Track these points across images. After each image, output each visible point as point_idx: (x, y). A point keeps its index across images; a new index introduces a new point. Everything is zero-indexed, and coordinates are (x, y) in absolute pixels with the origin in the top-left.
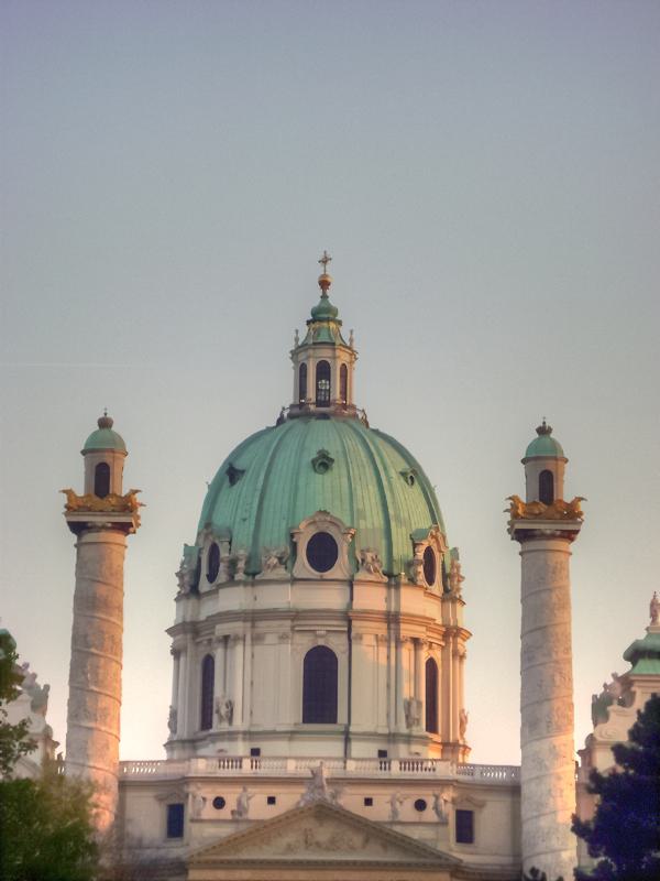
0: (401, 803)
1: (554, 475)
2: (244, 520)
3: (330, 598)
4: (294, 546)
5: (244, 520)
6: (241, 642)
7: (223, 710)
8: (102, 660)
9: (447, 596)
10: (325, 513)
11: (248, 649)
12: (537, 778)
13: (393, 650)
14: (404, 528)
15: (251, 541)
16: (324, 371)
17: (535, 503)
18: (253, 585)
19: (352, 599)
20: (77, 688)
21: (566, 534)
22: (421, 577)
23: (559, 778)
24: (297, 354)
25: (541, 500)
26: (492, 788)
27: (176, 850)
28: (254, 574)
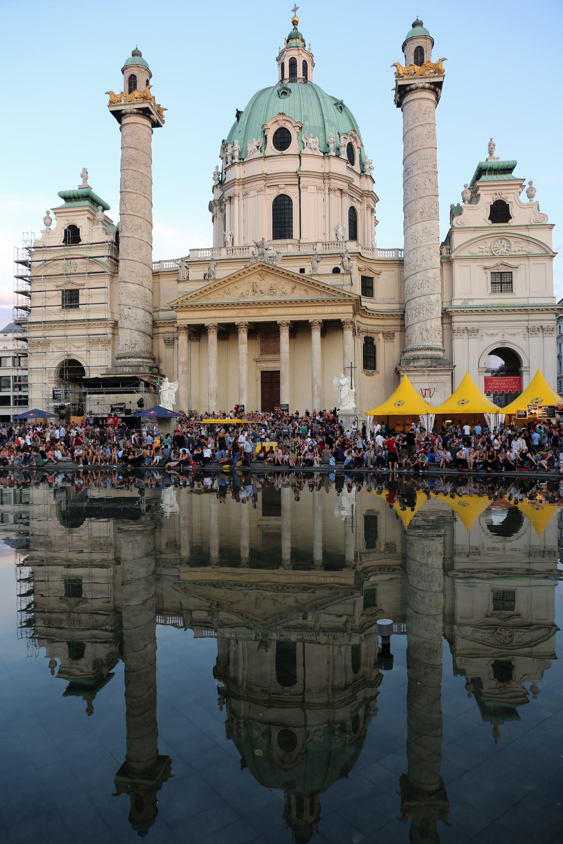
0: (317, 262)
4: (266, 137)
6: (237, 198)
8: (135, 195)
9: (362, 174)
10: (283, 114)
11: (241, 201)
12: (414, 249)
14: (334, 128)
15: (242, 142)
16: (293, 63)
17: (411, 65)
18: (243, 163)
19: (300, 165)
21: (432, 87)
22: (344, 156)
23: (429, 249)
24: (280, 59)
25: (415, 63)
26: (384, 262)
28: (243, 159)
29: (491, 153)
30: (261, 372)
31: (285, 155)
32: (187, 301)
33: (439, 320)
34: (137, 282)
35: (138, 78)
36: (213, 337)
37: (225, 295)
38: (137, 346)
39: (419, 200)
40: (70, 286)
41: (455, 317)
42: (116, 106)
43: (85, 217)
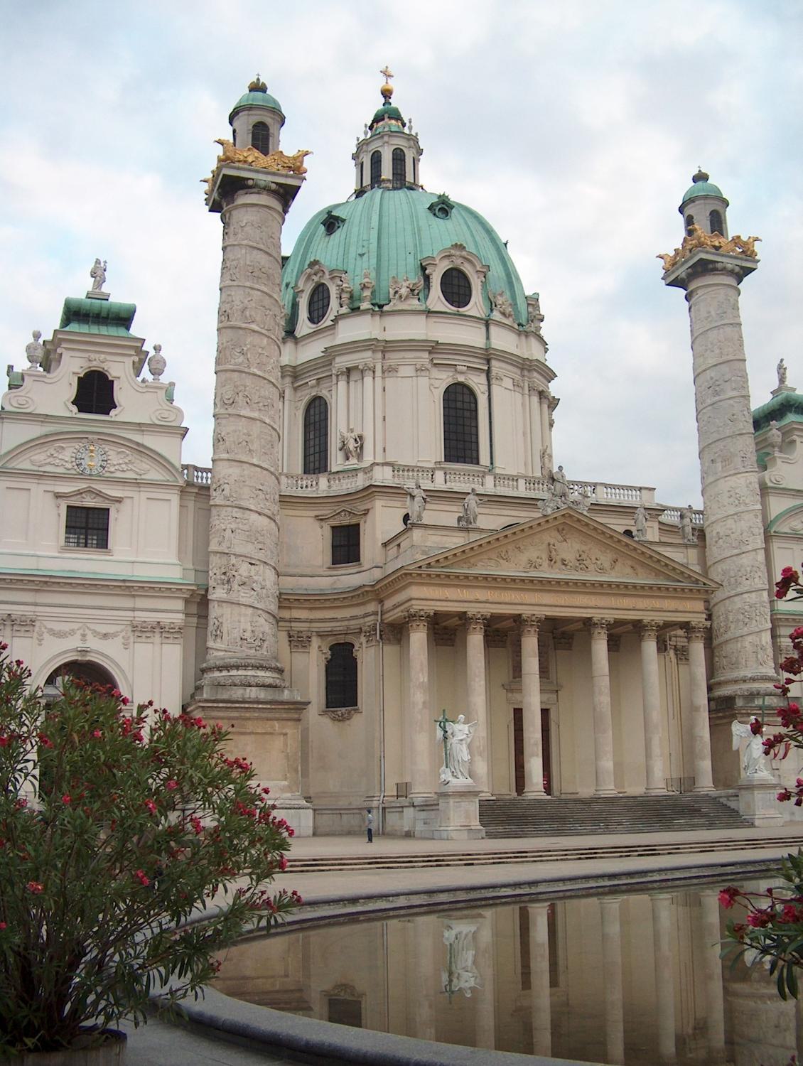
1: (723, 218)
2: (361, 255)
3: (471, 336)
4: (427, 278)
5: (364, 254)
7: (352, 445)
8: (265, 340)
11: (379, 381)
13: (527, 397)
16: (399, 157)
19: (488, 338)
20: (234, 371)
21: (742, 272)
24: (367, 144)
27: (349, 578)
28: (381, 307)
29: (782, 380)
30: (515, 709)
31: (465, 316)
32: (438, 565)
33: (769, 632)
34: (266, 511)
35: (271, 131)
36: (418, 638)
37: (501, 561)
38: (266, 644)
39: (738, 437)
40: (88, 499)
41: (781, 628)
42: (239, 168)
43: (129, 362)
